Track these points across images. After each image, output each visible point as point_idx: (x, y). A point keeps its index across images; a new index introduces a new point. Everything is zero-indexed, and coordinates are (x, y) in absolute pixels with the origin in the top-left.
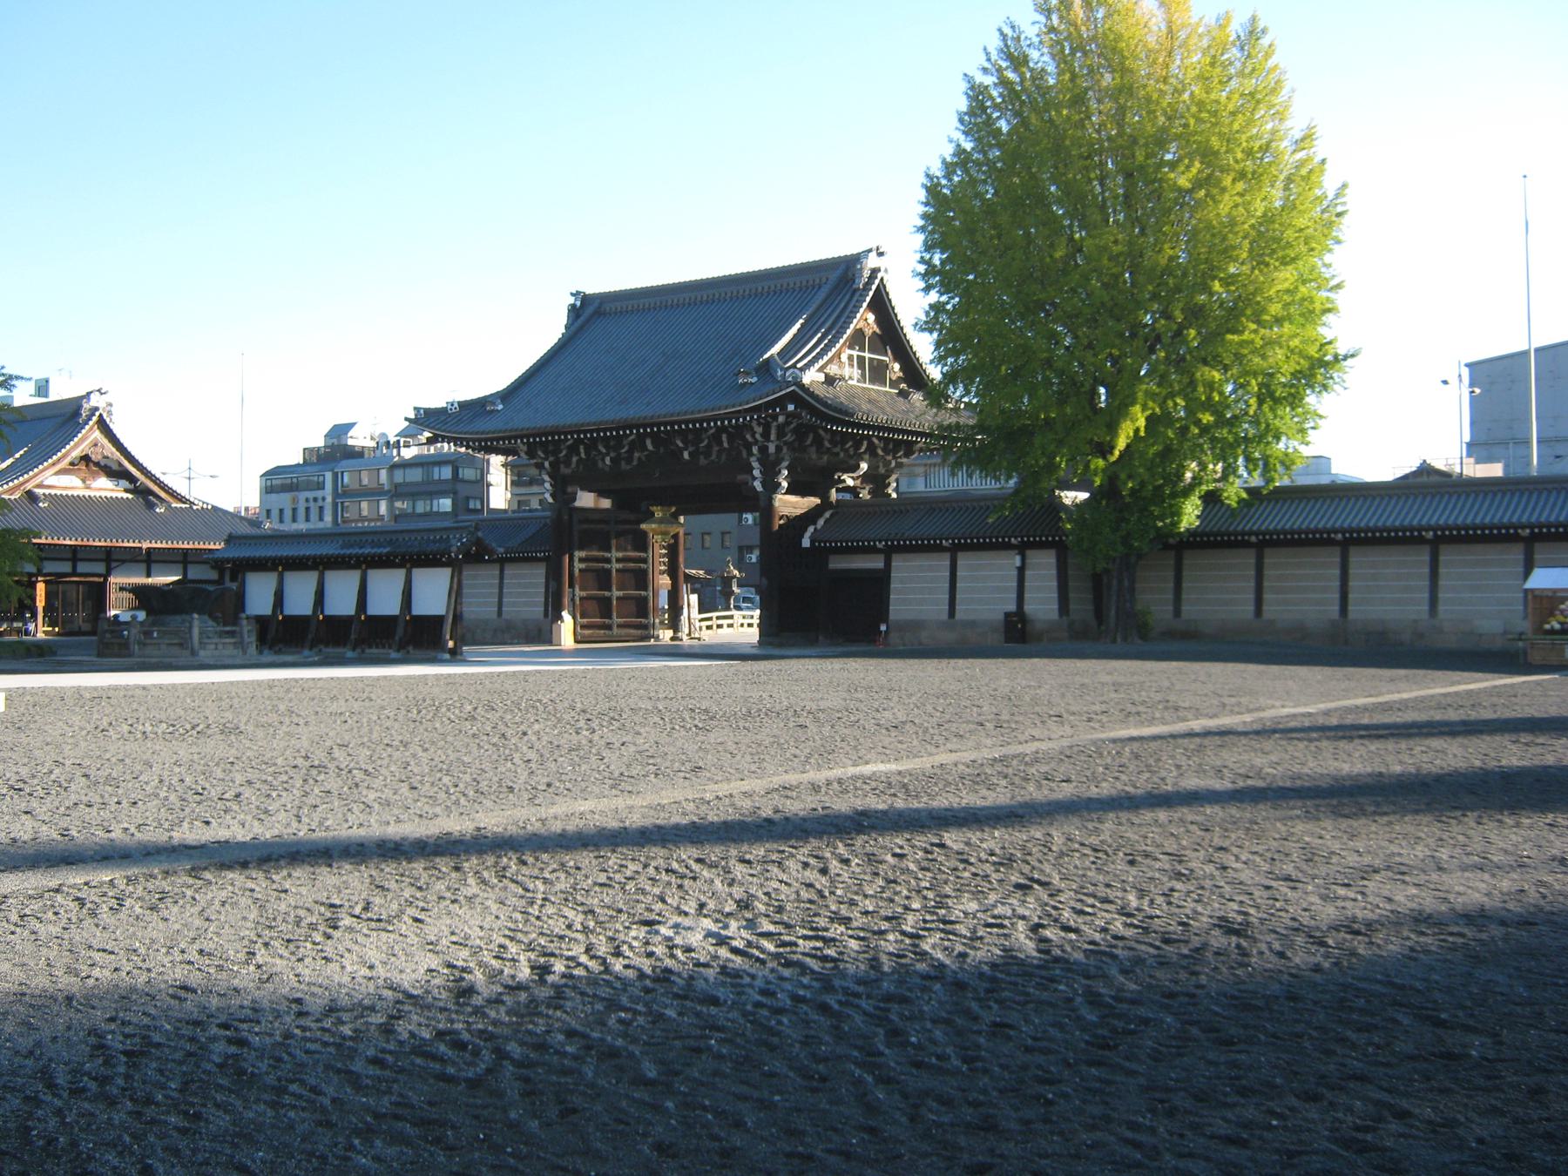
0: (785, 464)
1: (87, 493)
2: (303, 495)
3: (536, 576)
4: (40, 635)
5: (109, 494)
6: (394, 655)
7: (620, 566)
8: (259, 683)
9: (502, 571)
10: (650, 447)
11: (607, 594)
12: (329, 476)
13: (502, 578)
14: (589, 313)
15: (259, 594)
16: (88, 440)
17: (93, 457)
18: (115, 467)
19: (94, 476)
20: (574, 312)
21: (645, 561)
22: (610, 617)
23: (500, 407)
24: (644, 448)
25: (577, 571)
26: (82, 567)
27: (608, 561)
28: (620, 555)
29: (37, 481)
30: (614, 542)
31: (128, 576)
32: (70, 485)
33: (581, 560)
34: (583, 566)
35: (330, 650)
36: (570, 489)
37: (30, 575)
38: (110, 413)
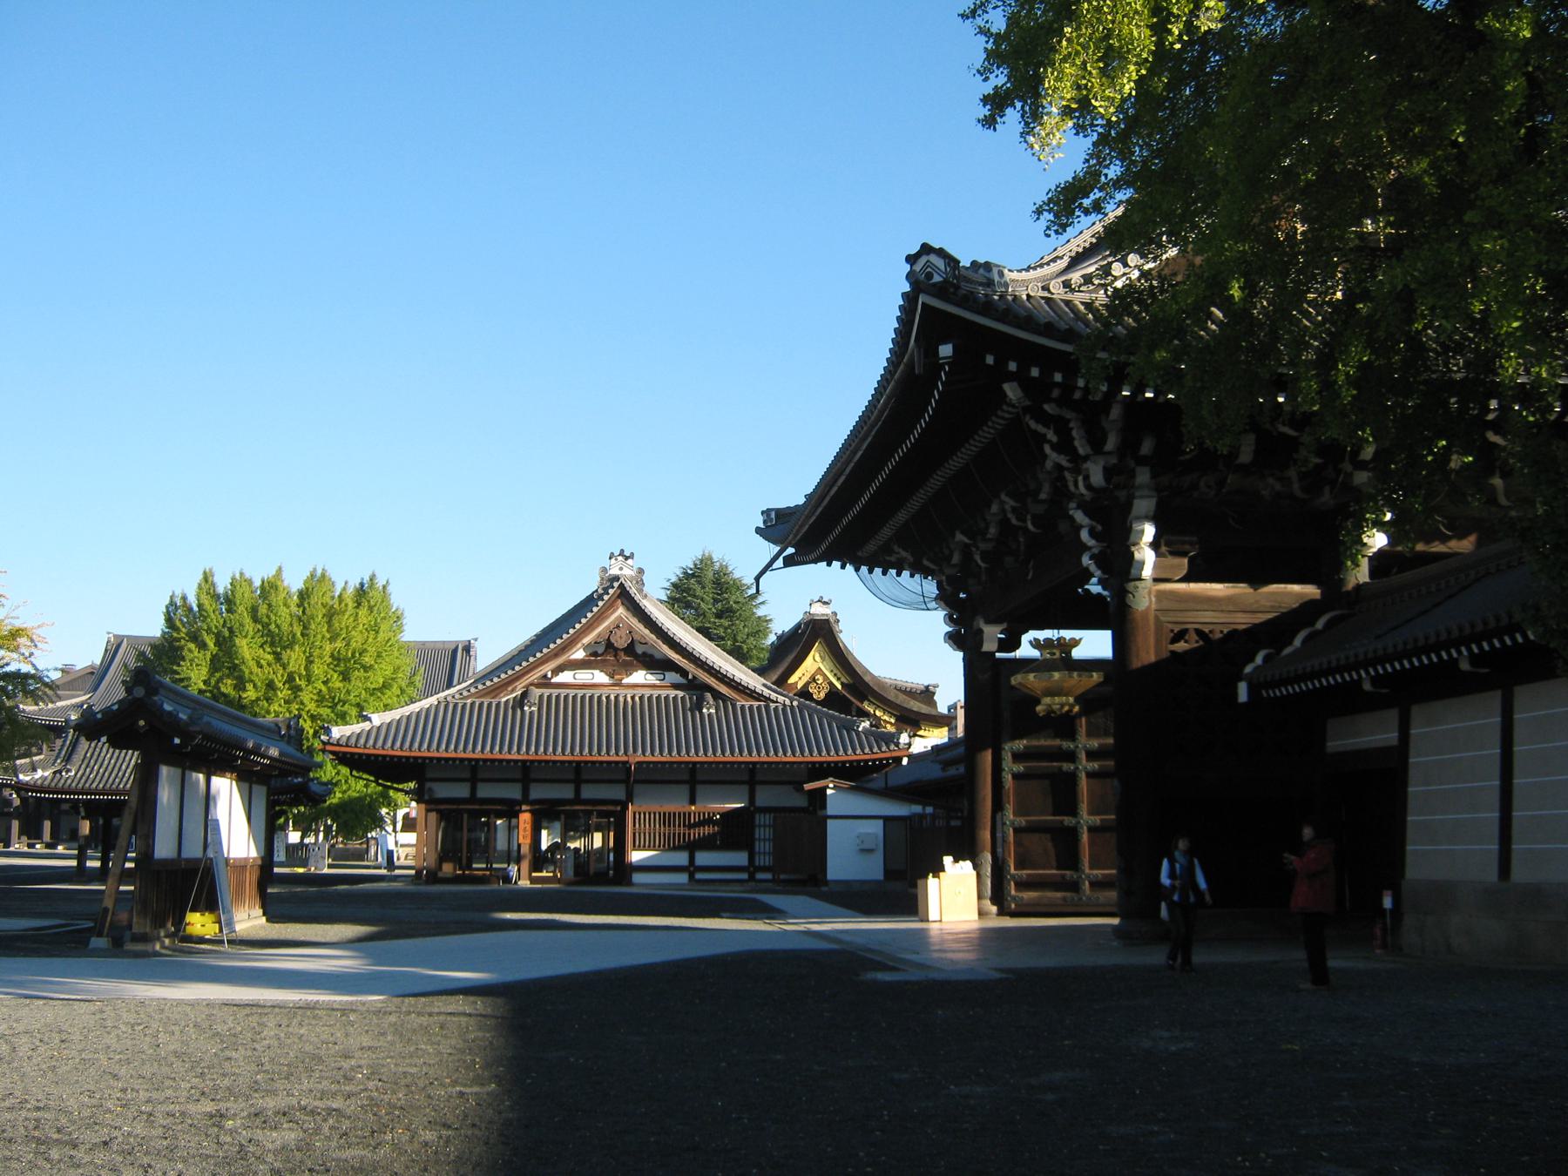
0: (1143, 504)
4: (524, 883)
5: (647, 692)
11: (1068, 821)
18: (657, 656)
19: (628, 669)
25: (1008, 779)
26: (588, 792)
27: (1071, 757)
28: (1095, 744)
29: (535, 676)
33: (1017, 757)
34: (1019, 768)
38: (640, 583)
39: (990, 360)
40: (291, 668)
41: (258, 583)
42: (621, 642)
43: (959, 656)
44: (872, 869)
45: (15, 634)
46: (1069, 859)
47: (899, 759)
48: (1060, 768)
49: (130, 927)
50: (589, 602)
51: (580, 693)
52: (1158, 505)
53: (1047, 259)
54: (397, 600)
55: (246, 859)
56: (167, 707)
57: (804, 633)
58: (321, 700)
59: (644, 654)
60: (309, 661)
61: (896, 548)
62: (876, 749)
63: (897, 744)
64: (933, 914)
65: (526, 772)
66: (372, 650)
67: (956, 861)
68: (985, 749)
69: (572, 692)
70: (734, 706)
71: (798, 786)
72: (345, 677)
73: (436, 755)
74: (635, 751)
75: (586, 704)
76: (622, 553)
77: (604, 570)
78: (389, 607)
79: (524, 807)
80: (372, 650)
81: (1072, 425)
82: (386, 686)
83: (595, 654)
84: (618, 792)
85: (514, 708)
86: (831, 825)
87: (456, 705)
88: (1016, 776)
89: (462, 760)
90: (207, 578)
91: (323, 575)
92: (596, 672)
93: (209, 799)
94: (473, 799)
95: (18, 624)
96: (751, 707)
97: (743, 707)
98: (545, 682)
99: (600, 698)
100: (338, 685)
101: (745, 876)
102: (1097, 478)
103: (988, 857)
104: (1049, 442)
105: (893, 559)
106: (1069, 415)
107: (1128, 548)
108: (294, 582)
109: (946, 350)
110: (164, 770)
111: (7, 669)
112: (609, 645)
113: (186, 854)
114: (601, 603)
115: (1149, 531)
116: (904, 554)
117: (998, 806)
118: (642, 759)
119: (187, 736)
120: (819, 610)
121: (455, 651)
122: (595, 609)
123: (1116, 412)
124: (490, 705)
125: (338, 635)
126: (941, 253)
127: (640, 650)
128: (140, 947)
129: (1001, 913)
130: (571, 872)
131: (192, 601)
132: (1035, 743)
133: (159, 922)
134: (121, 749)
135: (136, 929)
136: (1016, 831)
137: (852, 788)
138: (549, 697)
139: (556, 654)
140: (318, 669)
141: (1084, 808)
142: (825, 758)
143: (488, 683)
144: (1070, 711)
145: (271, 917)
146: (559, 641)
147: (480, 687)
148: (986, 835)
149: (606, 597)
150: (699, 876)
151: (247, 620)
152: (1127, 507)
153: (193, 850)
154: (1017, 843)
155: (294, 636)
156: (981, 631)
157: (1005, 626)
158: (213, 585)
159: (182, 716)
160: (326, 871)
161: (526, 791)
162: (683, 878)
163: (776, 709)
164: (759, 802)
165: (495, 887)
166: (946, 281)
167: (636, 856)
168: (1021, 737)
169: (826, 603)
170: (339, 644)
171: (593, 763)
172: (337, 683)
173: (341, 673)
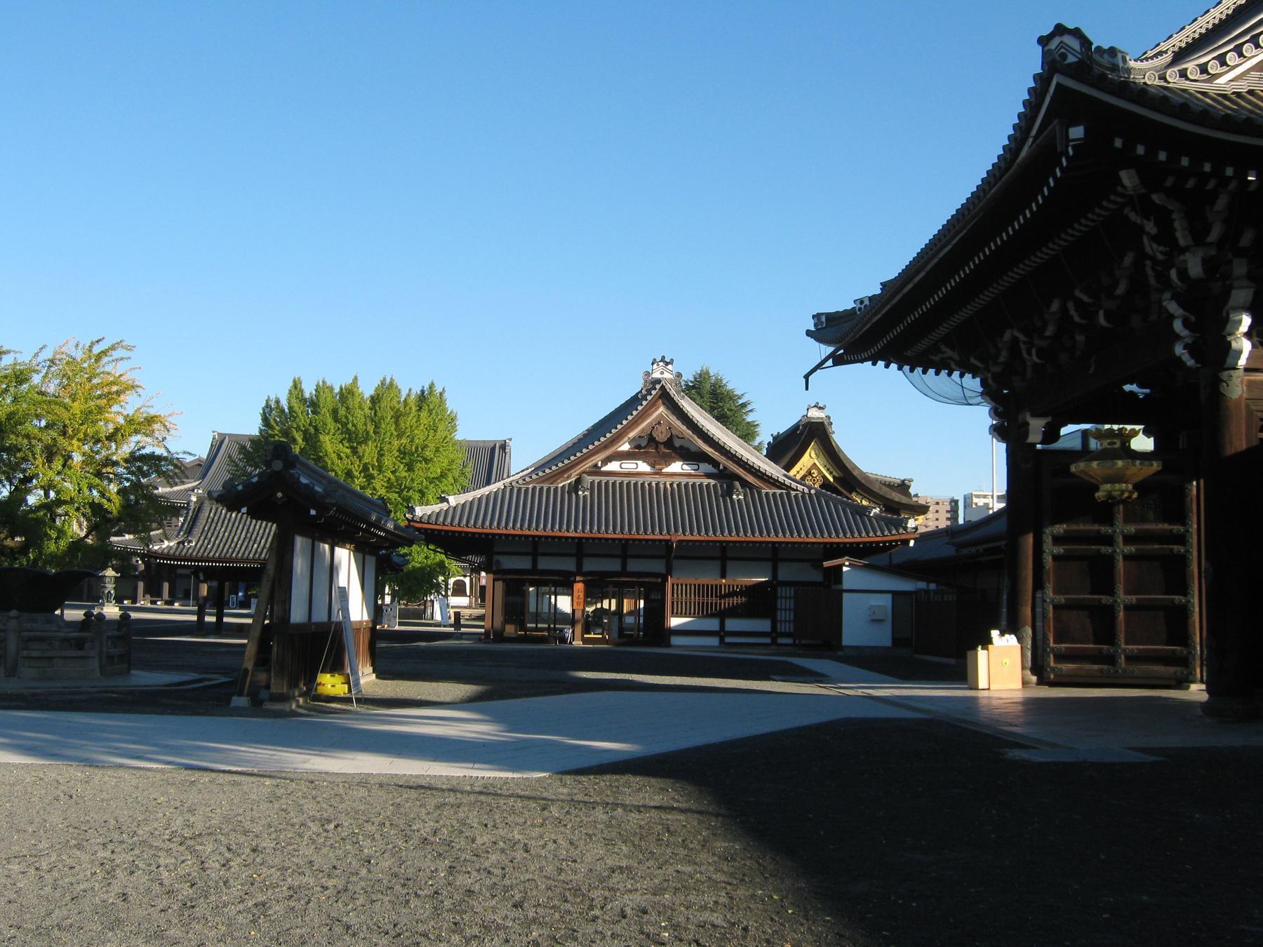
0: (1242, 295)
4: (578, 643)
5: (684, 480)
7: (1130, 549)
11: (1105, 599)
18: (693, 449)
19: (668, 460)
21: (1182, 539)
22: (1110, 639)
25: (1048, 560)
26: (634, 566)
27: (1109, 540)
28: (1131, 529)
29: (587, 465)
33: (1057, 540)
34: (1059, 550)
39: (1118, 143)
40: (365, 460)
41: (337, 390)
42: (661, 436)
43: (1002, 447)
44: (882, 637)
45: (150, 420)
46: (1106, 633)
47: (907, 541)
48: (1171, 550)
49: (268, 687)
50: (634, 401)
51: (626, 480)
52: (1256, 295)
53: (1150, 54)
54: (451, 405)
55: (361, 622)
56: (304, 480)
57: (802, 433)
58: (389, 488)
59: (681, 447)
60: (381, 455)
61: (943, 348)
62: (886, 533)
63: (905, 528)
64: (982, 683)
65: (580, 548)
66: (432, 446)
67: (1002, 634)
68: (1027, 532)
69: (619, 480)
70: (759, 493)
71: (817, 564)
72: (410, 468)
73: (504, 532)
74: (676, 530)
75: (630, 489)
76: (663, 360)
77: (648, 374)
78: (445, 410)
79: (578, 578)
80: (432, 446)
81: (1174, 216)
82: (444, 475)
83: (638, 447)
84: (658, 566)
85: (569, 492)
86: (845, 595)
87: (519, 490)
88: (1056, 558)
89: (527, 537)
90: (296, 385)
91: (391, 384)
92: (640, 463)
93: (332, 569)
94: (534, 570)
95: (152, 412)
96: (774, 494)
97: (767, 494)
98: (595, 471)
99: (643, 484)
100: (404, 474)
101: (768, 640)
102: (1195, 269)
103: (1029, 631)
104: (1148, 233)
105: (937, 358)
106: (1172, 206)
107: (1225, 337)
108: (367, 390)
109: (1077, 132)
110: (299, 542)
111: (143, 452)
112: (651, 439)
113: (315, 619)
114: (644, 403)
115: (1246, 321)
116: (949, 353)
117: (1038, 585)
118: (682, 538)
119: (322, 508)
120: (815, 414)
121: (493, 449)
122: (640, 408)
123: (1221, 203)
124: (549, 489)
125: (404, 433)
126: (1077, 33)
127: (677, 443)
128: (278, 707)
129: (1041, 682)
130: (616, 635)
131: (284, 404)
132: (1074, 527)
133: (294, 684)
134: (262, 520)
135: (274, 690)
136: (1055, 607)
137: (865, 566)
138: (599, 483)
139: (606, 446)
140: (388, 461)
141: (1120, 589)
142: (842, 539)
143: (548, 471)
144: (1129, 497)
145: (381, 673)
146: (608, 435)
147: (541, 474)
148: (1027, 611)
149: (649, 398)
150: (728, 640)
151: (330, 420)
152: (1226, 295)
153: (320, 616)
155: (368, 433)
156: (1027, 424)
157: (1049, 419)
158: (302, 391)
159: (318, 489)
160: (397, 628)
161: (579, 565)
162: (714, 641)
163: (796, 496)
164: (781, 577)
165: (552, 646)
166: (1081, 62)
167: (675, 622)
168: (1061, 522)
169: (821, 408)
170: (404, 441)
171: (640, 540)
172: (403, 473)
173: (406, 464)
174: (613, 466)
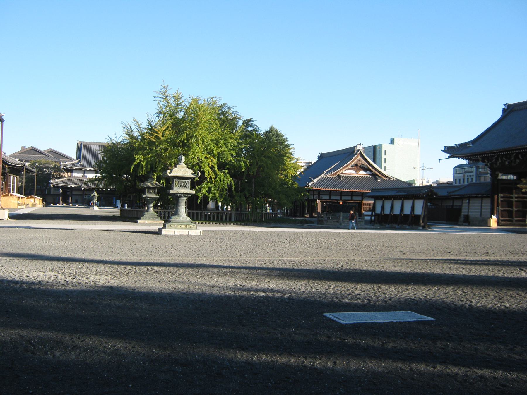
1: (357, 175)
2: (466, 174)
3: (487, 203)
5: (364, 176)
6: (408, 227)
7: (516, 199)
8: (336, 233)
9: (482, 201)
10: (520, 158)
11: (511, 209)
12: (475, 169)
13: (482, 203)
14: (509, 110)
15: (419, 207)
16: (357, 159)
17: (359, 165)
18: (366, 167)
19: (359, 170)
20: (504, 110)
22: (512, 217)
23: (471, 145)
24: (518, 158)
25: (500, 201)
26: (354, 198)
27: (512, 198)
28: (516, 195)
29: (341, 172)
30: (514, 191)
31: (368, 200)
32: (352, 172)
33: (502, 197)
34: (502, 199)
35: (394, 225)
36: (496, 173)
37: (337, 200)
88: (501, 201)
139: (346, 167)
141: (514, 207)
154: (501, 213)
161: (341, 198)
174: (346, 172)
